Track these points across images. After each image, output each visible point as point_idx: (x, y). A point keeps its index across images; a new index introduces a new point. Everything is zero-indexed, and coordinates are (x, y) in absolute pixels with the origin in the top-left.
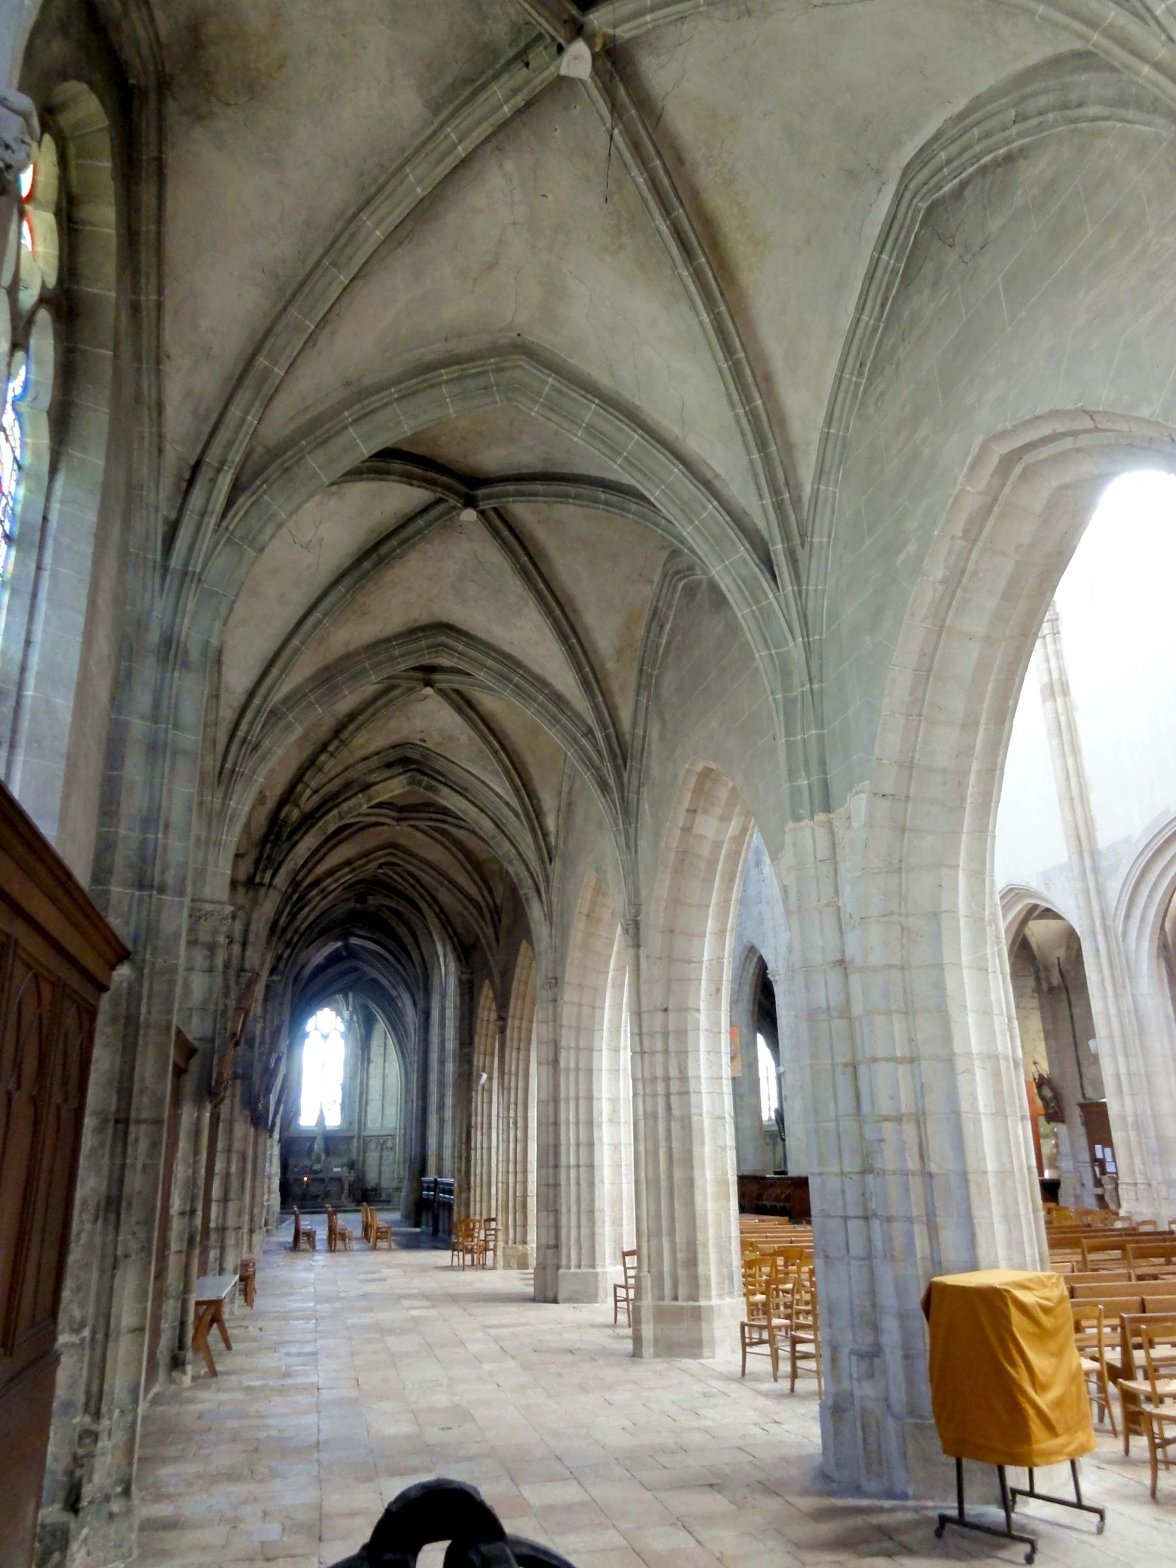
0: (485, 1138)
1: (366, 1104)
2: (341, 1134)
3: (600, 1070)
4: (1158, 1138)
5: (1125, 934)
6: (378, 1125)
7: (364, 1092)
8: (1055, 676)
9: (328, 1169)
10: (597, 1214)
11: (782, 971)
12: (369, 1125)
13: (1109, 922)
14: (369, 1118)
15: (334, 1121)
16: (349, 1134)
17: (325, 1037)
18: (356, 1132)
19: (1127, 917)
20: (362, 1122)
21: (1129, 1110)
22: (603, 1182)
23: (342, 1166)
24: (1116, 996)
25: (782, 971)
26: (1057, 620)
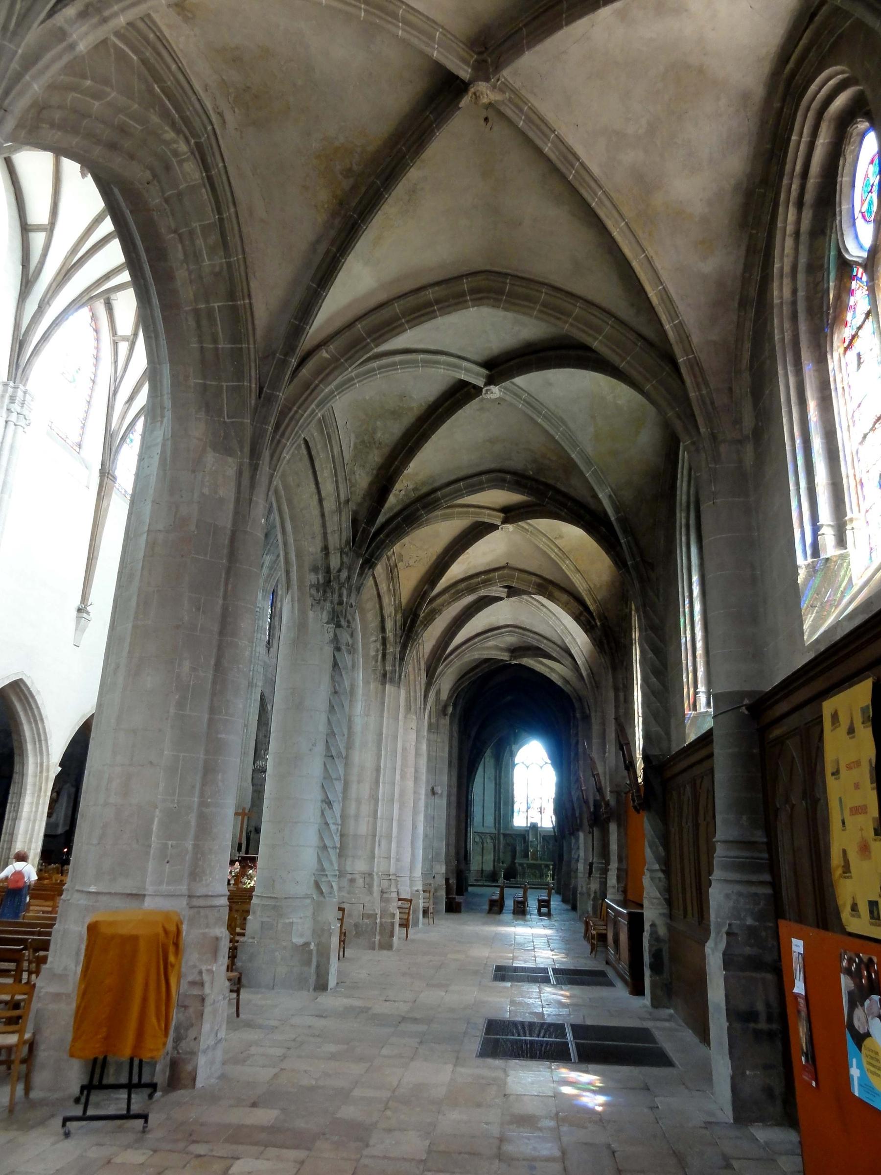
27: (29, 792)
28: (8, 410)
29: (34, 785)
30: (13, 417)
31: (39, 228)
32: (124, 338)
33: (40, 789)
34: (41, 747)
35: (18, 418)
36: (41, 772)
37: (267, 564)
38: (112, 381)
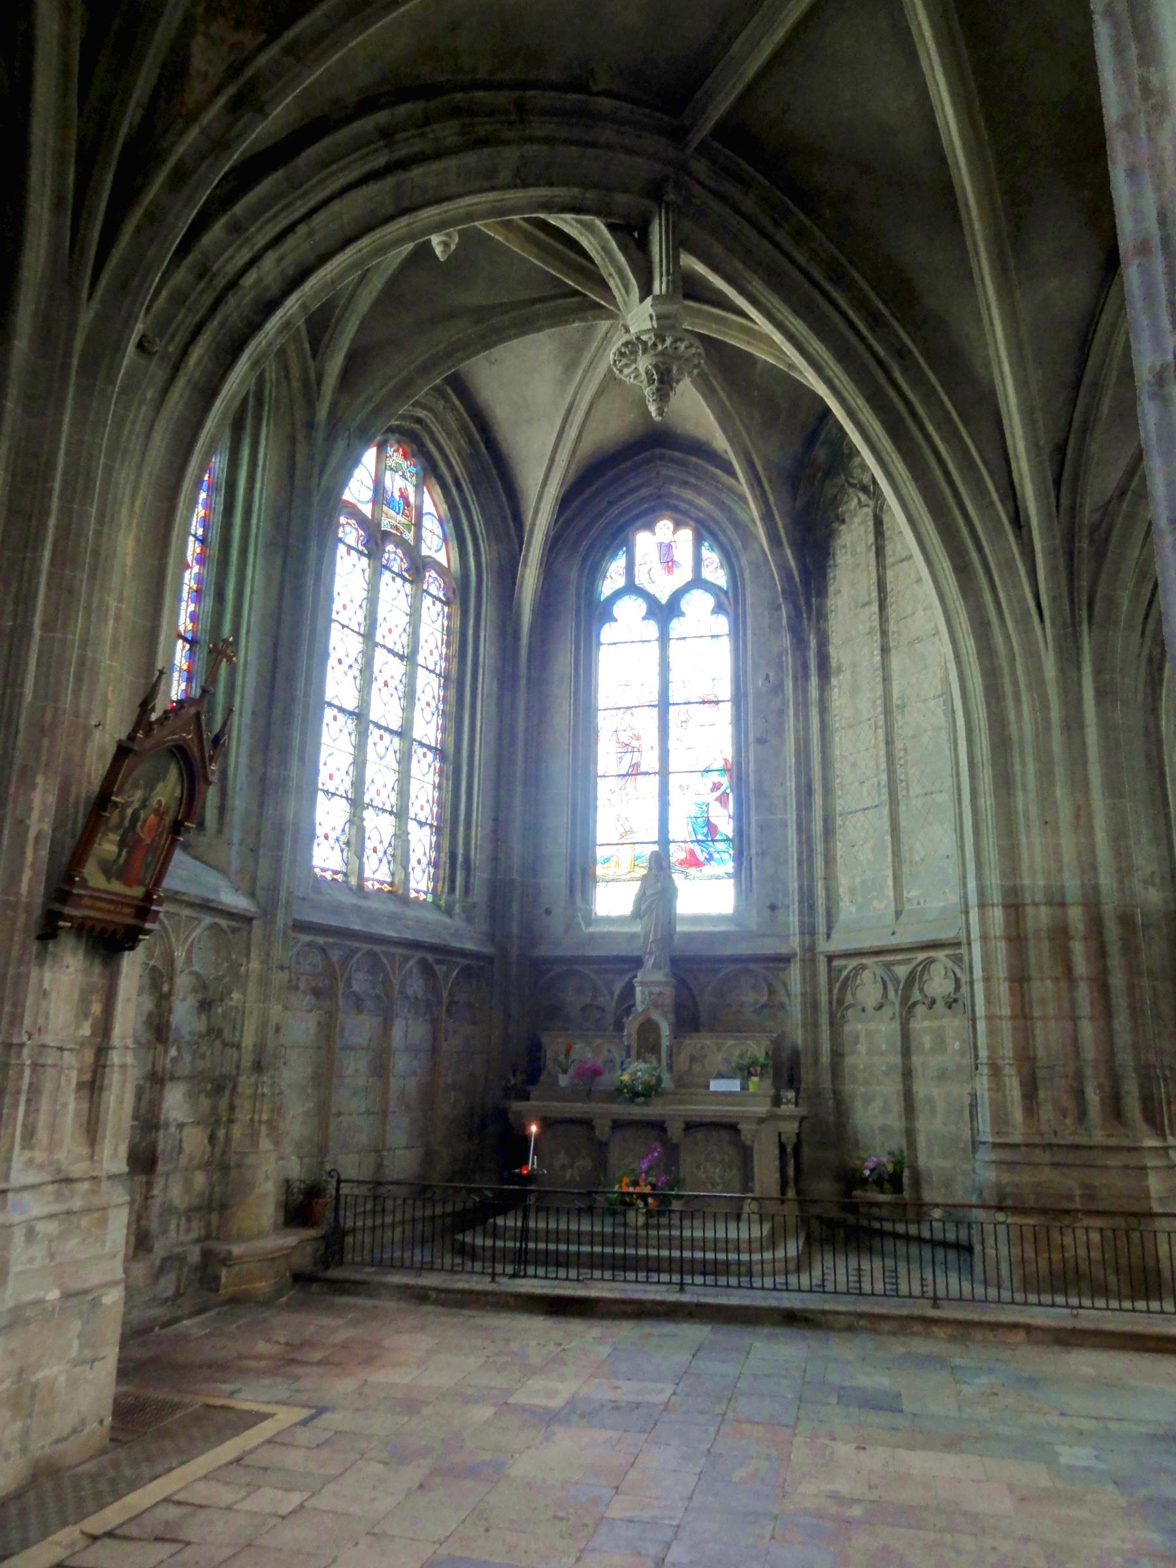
1: (829, 831)
2: (745, 949)
6: (884, 904)
7: (814, 784)
9: (690, 1083)
12: (847, 910)
14: (843, 883)
15: (708, 896)
16: (770, 947)
17: (664, 612)
18: (795, 943)
20: (817, 906)
23: (746, 1071)
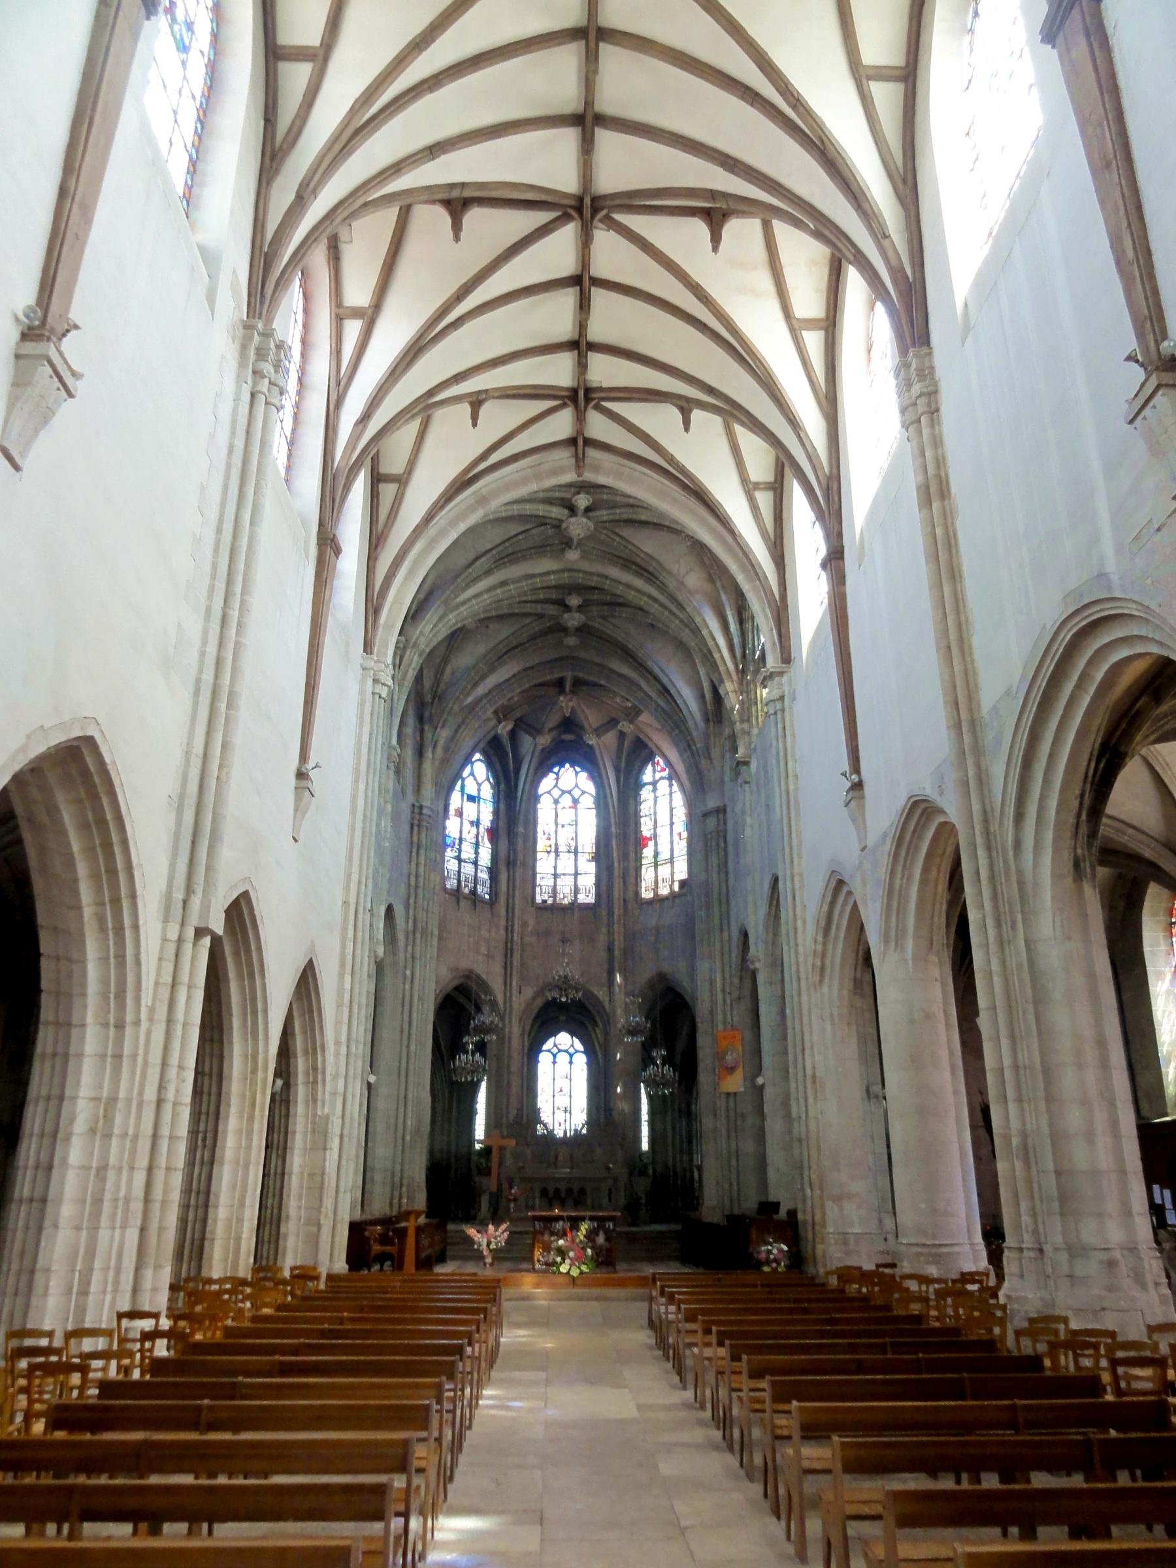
0: (280, 1163)
3: (80, 1055)
4: (1058, 1173)
5: (1018, 844)
8: (931, 471)
10: (38, 1276)
11: (761, 957)
13: (994, 827)
19: (1019, 817)
21: (1015, 1124)
22: (56, 1226)
24: (1001, 944)
25: (761, 957)
26: (936, 392)
27: (233, 1110)
28: (254, 372)
29: (243, 1096)
30: (264, 385)
31: (301, 54)
32: (357, 313)
33: (253, 1105)
34: (255, 1023)
35: (269, 391)
36: (254, 1071)
37: (441, 743)
38: (333, 384)
